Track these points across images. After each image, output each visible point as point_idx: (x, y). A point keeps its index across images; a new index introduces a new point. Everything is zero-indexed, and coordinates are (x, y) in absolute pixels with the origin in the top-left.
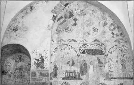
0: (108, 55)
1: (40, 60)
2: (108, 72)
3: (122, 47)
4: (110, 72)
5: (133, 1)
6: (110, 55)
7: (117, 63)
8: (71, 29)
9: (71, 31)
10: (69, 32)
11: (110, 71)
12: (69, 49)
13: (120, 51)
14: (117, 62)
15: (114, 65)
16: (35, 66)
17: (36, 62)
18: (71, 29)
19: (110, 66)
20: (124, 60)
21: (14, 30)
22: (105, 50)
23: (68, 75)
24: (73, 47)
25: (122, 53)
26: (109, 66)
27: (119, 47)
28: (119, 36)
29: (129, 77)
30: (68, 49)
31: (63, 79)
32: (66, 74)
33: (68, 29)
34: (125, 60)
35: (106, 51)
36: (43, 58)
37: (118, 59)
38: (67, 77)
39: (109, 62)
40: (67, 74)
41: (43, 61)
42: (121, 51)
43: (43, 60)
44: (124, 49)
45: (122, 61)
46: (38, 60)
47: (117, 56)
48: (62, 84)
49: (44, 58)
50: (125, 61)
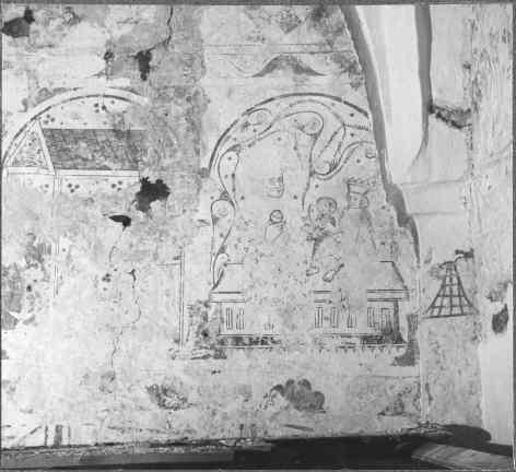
0: (214, 173)
2: (204, 298)
3: (309, 106)
4: (217, 297)
6: (227, 164)
7: (273, 231)
11: (219, 289)
13: (305, 139)
14: (277, 219)
15: (252, 249)
20: (332, 203)
22: (192, 136)
25: (316, 152)
26: (216, 251)
27: (298, 107)
28: (304, 26)
35: (196, 141)
39: (215, 220)
42: (315, 137)
44: (332, 125)
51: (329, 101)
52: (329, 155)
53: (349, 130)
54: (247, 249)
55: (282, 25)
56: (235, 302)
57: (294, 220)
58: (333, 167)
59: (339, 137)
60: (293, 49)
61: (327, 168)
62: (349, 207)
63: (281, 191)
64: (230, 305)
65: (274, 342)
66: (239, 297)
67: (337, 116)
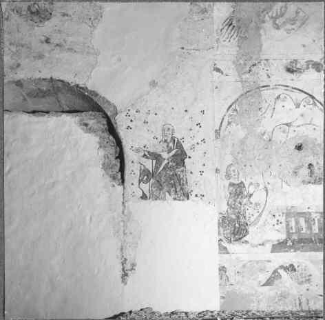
1: (165, 155)
5: (323, 3)
8: (297, 13)
9: (298, 23)
10: (289, 26)
12: (298, 106)
16: (146, 187)
17: (149, 164)
18: (297, 13)
21: (35, 18)
23: (299, 230)
24: (313, 98)
30: (289, 105)
31: (280, 246)
32: (293, 224)
33: (282, 15)
36: (179, 146)
38: (295, 237)
40: (297, 223)
41: (183, 161)
43: (180, 157)
46: (157, 157)
48: (275, 271)
49: (186, 146)
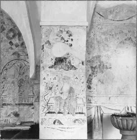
3: (21, 62)
5: (1, 1)
7: (12, 84)
19: (3, 88)
20: (23, 80)
25: (21, 70)
27: (18, 62)
28: (19, 47)
29: (27, 102)
34: (24, 80)
37: (15, 79)
42: (21, 67)
45: (19, 82)
47: (14, 75)
50: (23, 82)
51: (23, 61)
52: (23, 71)
53: (26, 66)
54: (8, 88)
55: (16, 46)
56: (5, 97)
57: (16, 83)
58: (23, 73)
59: (25, 67)
60: (17, 51)
61: (22, 73)
62: (25, 80)
63: (14, 77)
64: (4, 98)
65: (12, 105)
66: (5, 96)
67: (25, 64)
